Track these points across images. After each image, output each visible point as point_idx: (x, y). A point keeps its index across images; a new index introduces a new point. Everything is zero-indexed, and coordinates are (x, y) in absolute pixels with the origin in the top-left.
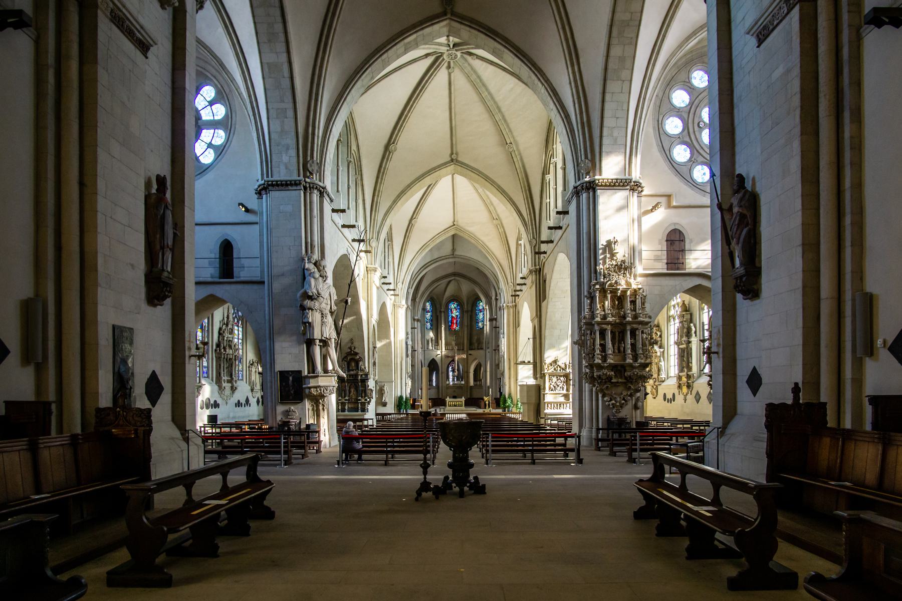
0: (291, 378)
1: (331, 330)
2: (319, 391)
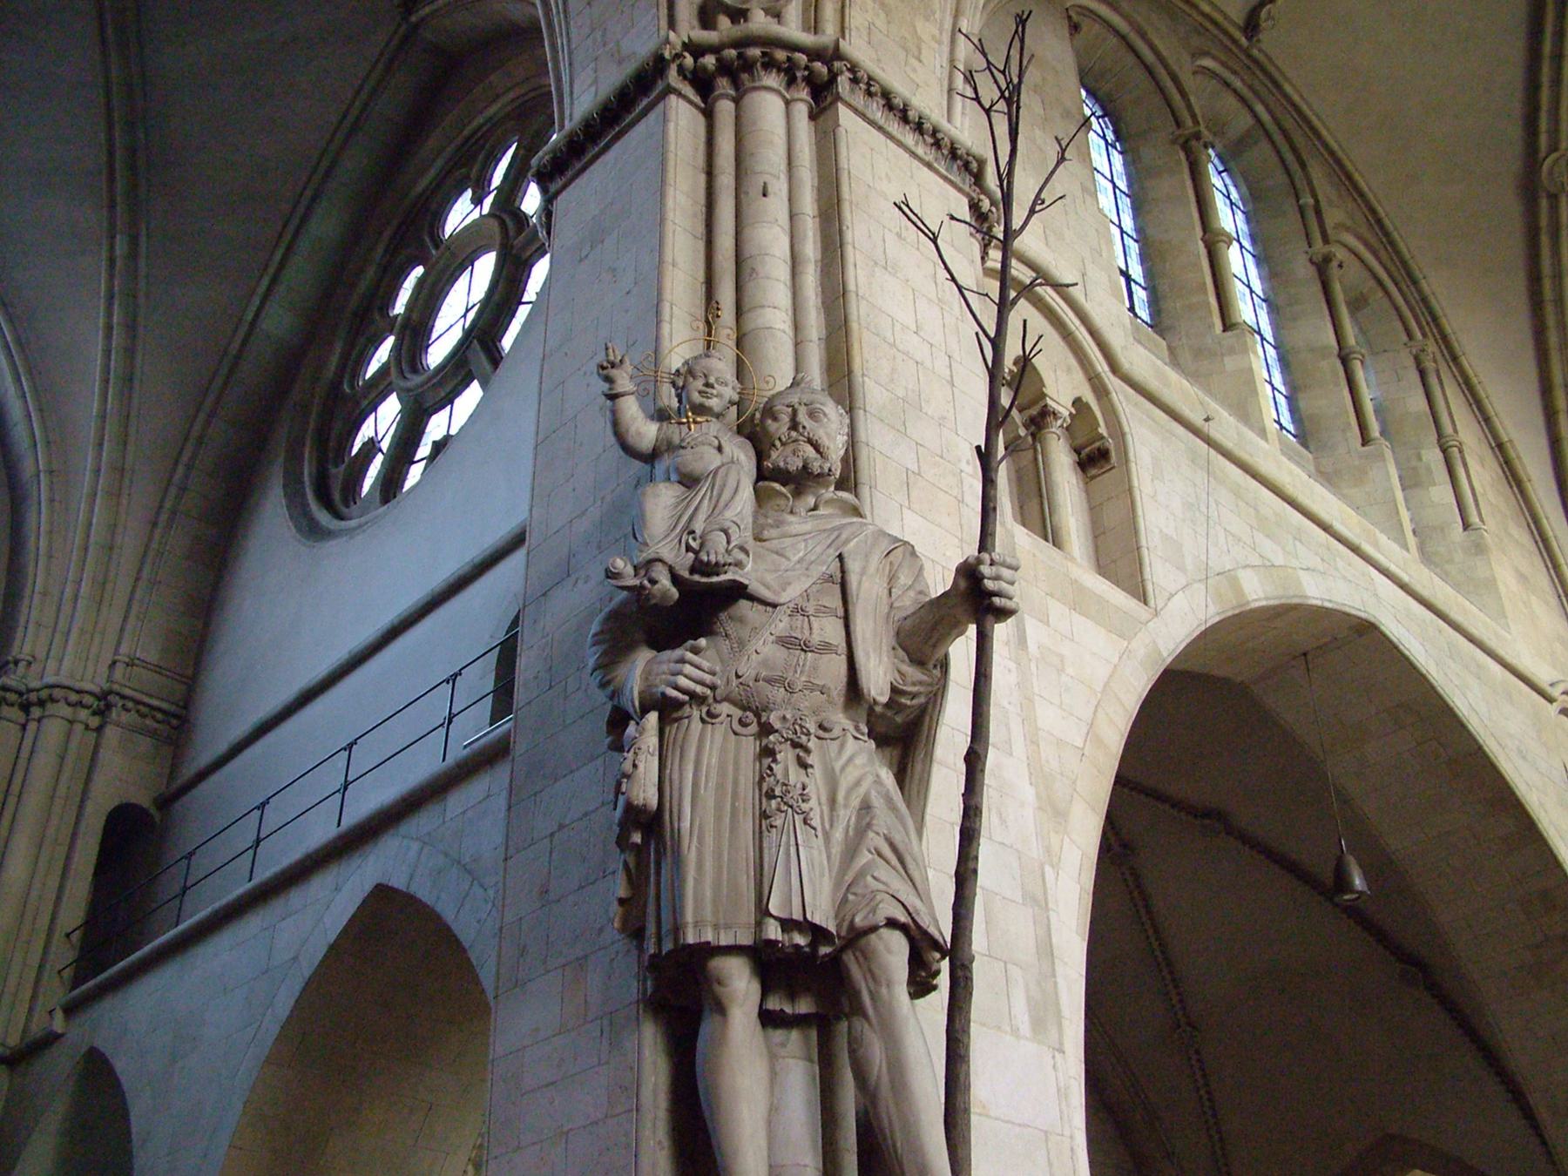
1: (865, 857)
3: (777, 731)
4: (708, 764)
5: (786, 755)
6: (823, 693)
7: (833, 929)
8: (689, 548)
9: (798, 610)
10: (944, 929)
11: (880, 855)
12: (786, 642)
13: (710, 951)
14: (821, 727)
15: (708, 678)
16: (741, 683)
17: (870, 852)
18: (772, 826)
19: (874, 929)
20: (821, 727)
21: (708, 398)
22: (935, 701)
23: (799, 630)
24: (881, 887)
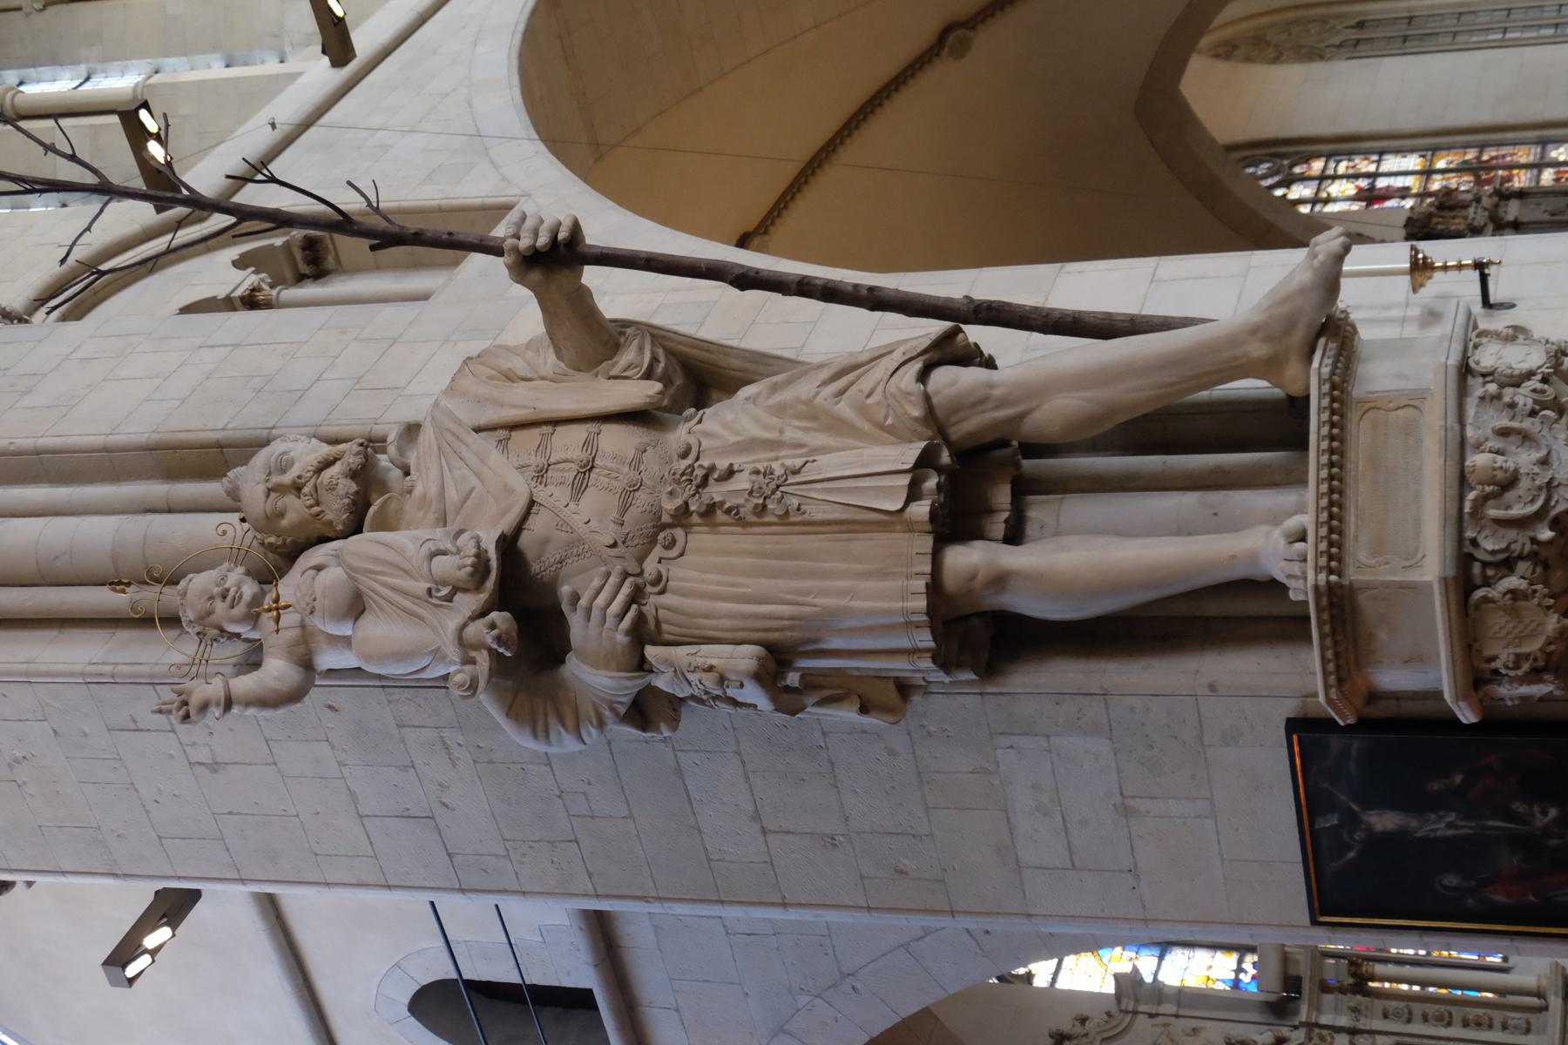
0: (1385, 821)
1: (844, 409)
2: (1513, 582)
3: (686, 503)
4: (719, 584)
5: (715, 492)
6: (645, 451)
7: (923, 444)
8: (449, 598)
9: (541, 474)
10: (934, 328)
11: (842, 392)
12: (579, 488)
13: (935, 587)
14: (684, 455)
15: (613, 580)
16: (624, 542)
17: (837, 403)
18: (799, 509)
19: (927, 398)
20: (684, 455)
21: (241, 597)
22: (663, 337)
23: (566, 474)
24: (880, 389)
